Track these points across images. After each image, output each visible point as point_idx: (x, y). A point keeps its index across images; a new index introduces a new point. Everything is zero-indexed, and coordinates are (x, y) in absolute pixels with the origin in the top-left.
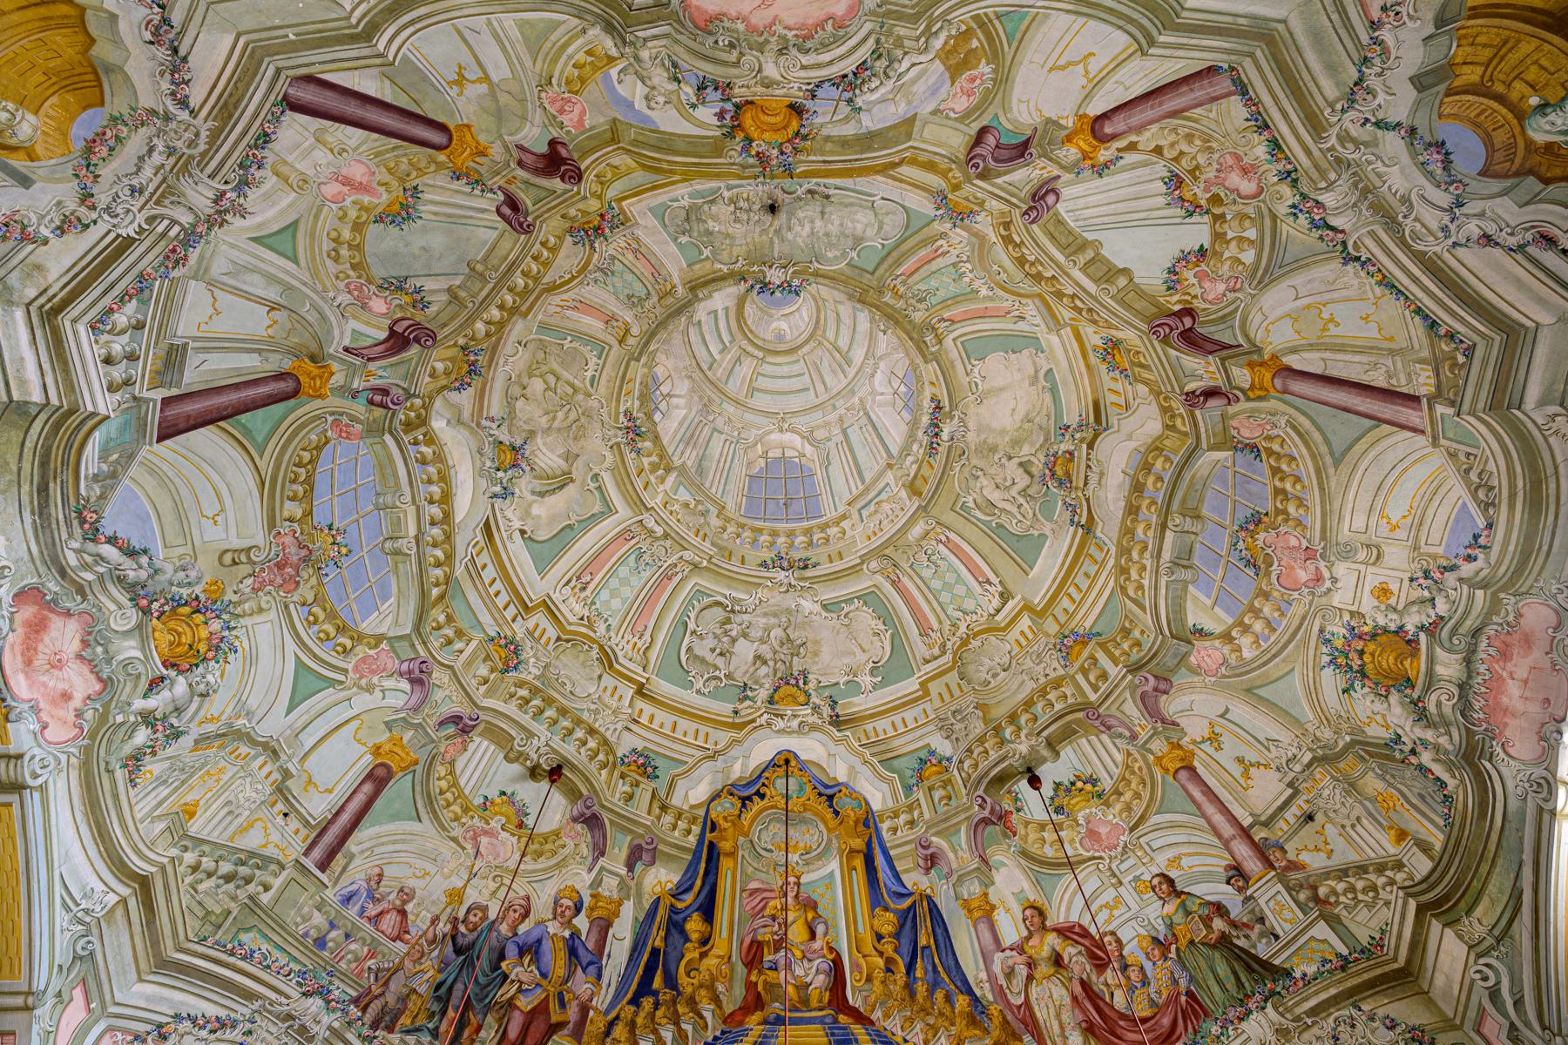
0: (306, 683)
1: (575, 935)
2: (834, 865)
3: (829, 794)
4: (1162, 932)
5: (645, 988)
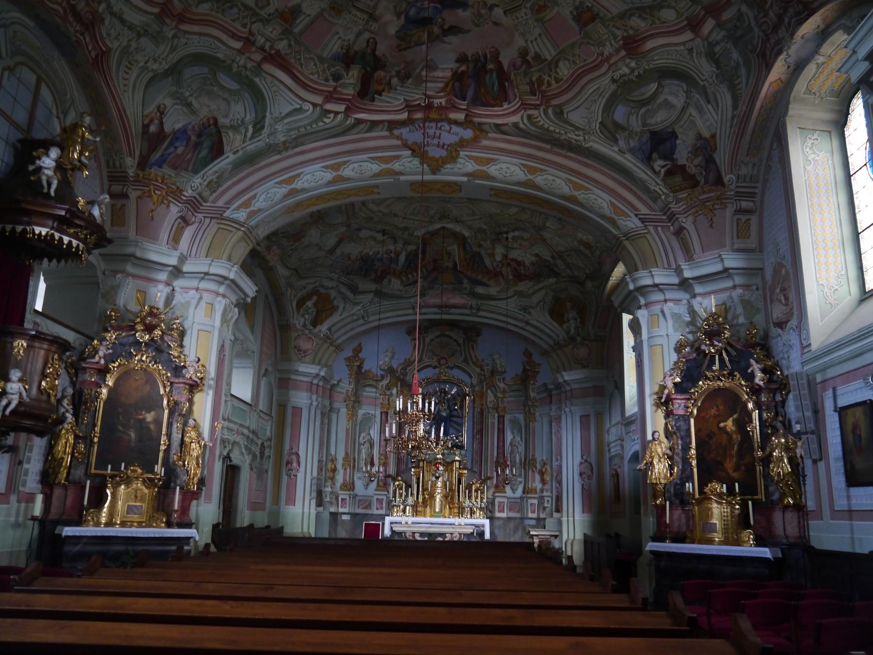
1: (391, 257)
2: (456, 247)
3: (455, 235)
4: (534, 262)
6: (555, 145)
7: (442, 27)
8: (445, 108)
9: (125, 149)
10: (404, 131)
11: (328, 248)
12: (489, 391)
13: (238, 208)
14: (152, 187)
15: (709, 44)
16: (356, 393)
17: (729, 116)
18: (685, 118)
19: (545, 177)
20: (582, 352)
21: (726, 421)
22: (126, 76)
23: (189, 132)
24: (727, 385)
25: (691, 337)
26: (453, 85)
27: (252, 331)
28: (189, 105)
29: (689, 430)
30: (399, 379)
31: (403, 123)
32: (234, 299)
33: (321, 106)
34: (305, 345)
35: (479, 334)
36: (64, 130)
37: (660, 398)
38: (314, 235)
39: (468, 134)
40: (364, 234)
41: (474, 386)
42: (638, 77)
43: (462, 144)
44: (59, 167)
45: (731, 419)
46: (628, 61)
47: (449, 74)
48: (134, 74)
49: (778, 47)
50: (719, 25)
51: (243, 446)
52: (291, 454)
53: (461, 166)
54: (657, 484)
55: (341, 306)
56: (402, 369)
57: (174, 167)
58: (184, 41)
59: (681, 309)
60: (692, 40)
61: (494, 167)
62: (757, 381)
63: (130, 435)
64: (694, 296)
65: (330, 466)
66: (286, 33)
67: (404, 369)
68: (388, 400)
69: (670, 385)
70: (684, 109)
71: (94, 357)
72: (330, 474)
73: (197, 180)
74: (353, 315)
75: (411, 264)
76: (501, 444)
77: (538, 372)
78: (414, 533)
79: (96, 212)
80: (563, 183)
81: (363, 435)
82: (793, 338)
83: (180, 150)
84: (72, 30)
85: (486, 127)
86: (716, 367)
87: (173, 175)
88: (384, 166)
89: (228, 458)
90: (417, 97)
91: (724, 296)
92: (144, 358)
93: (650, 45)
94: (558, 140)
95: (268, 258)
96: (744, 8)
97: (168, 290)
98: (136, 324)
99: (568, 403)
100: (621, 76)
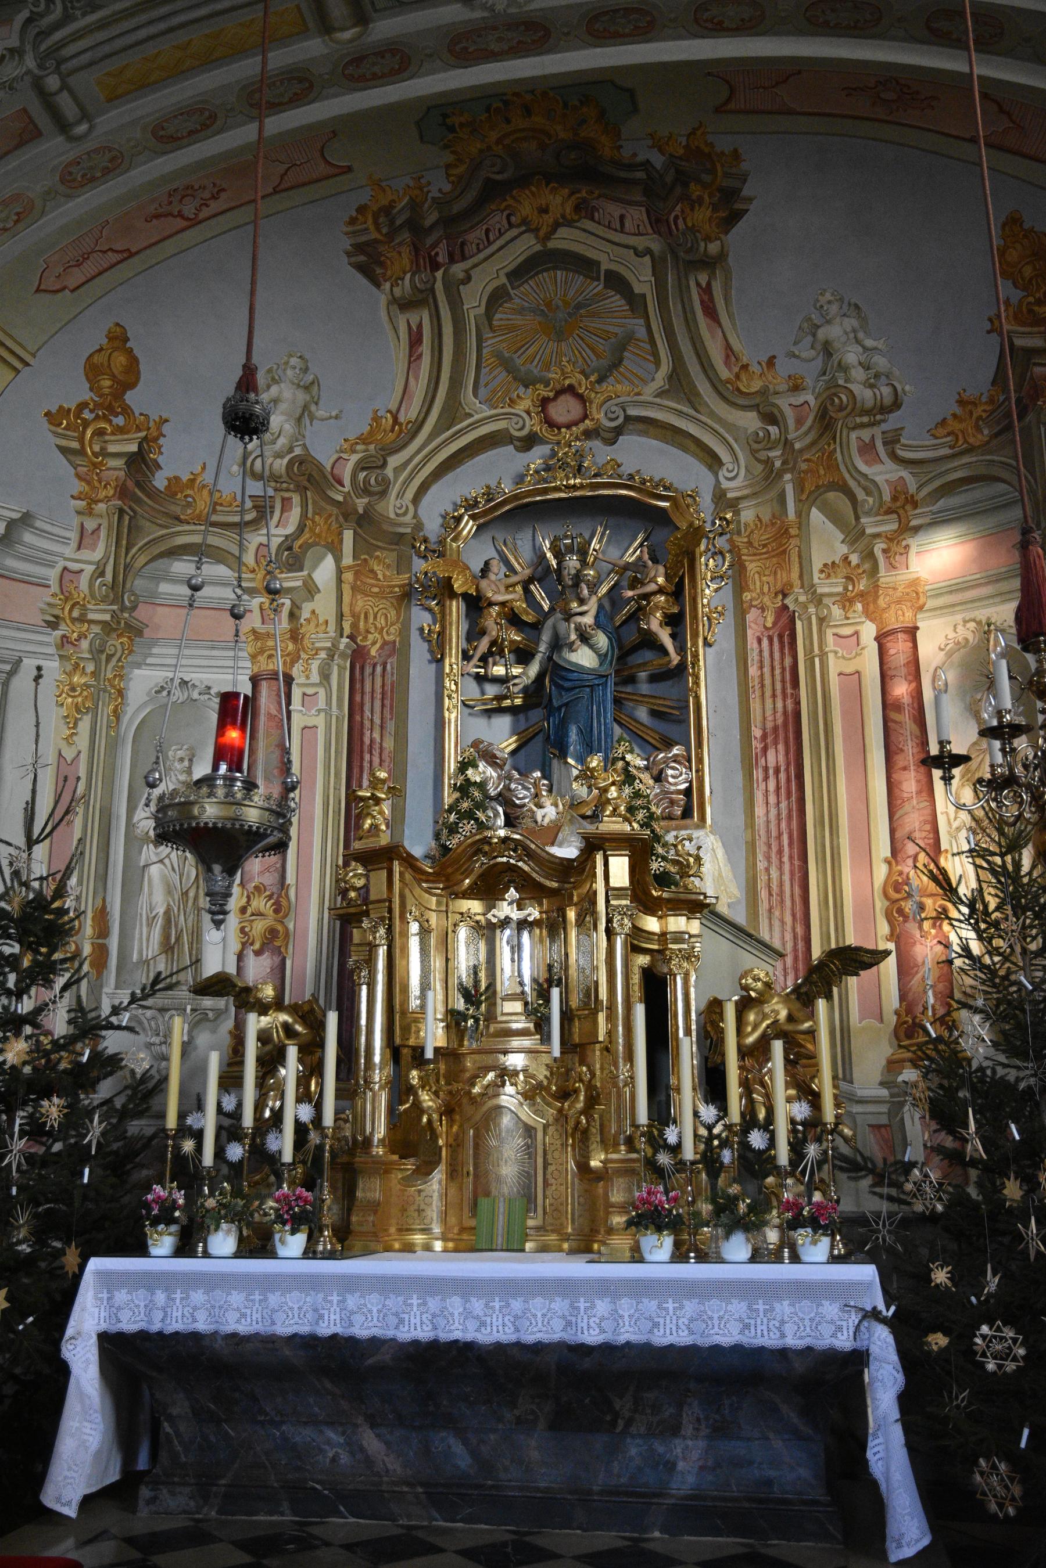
12: (816, 515)
16: (117, 591)
30: (347, 512)
41: (734, 505)
56: (361, 466)
67: (372, 464)
68: (293, 616)
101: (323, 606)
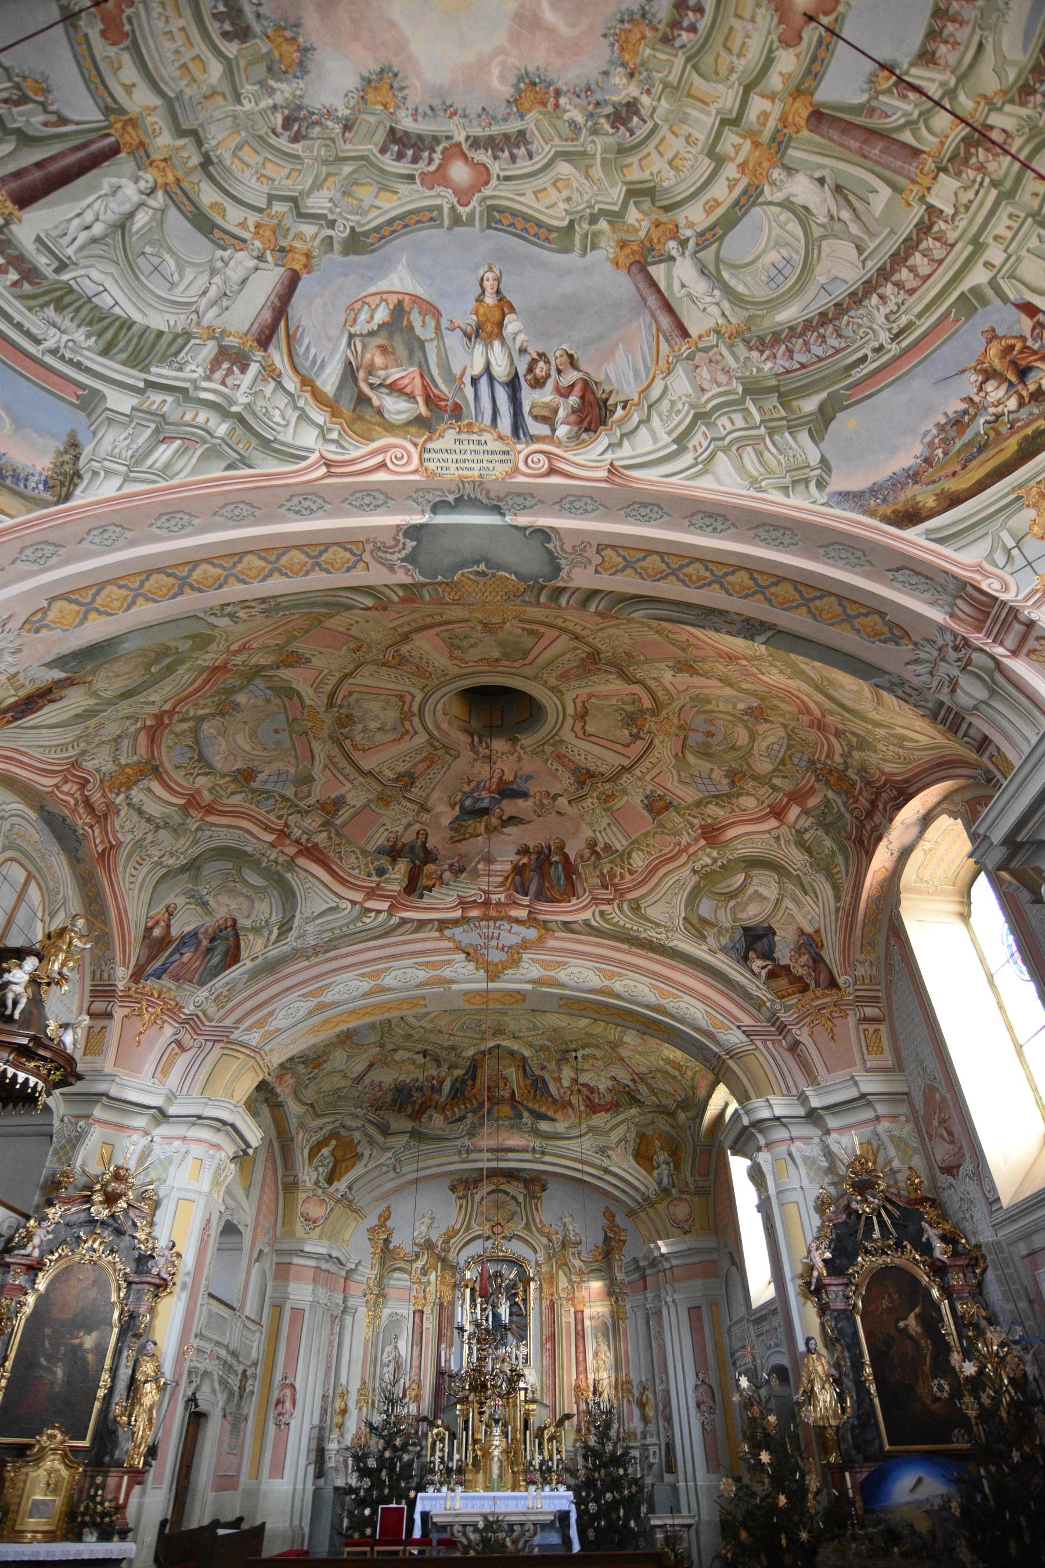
0: (349, 1058)
2: (513, 1069)
3: (512, 1053)
5: (455, 1096)
6: (633, 945)
7: (500, 818)
8: (506, 904)
9: (118, 957)
10: (457, 931)
11: (354, 1075)
13: (249, 1029)
14: (144, 1003)
15: (797, 831)
16: (380, 1284)
17: (833, 908)
18: (781, 913)
19: (625, 982)
20: (681, 1211)
21: (906, 1318)
22: (134, 872)
23: (201, 936)
24: (897, 1261)
25: (832, 1190)
26: (513, 880)
27: (247, 1196)
28: (204, 904)
29: (856, 1333)
30: (439, 1256)
31: (456, 922)
32: (230, 1149)
33: (361, 903)
34: (316, 1211)
35: (544, 1188)
36: (49, 936)
37: (808, 1284)
38: (339, 1058)
39: (532, 933)
40: (400, 1055)
42: (722, 867)
43: (525, 945)
44: (34, 981)
45: (912, 1315)
46: (708, 850)
47: (508, 867)
48: (145, 869)
49: (875, 834)
50: (806, 812)
51: (216, 1378)
52: (284, 1386)
53: (524, 972)
54: (825, 1427)
55: (367, 1153)
57: (177, 978)
58: (209, 833)
59: (814, 1150)
60: (778, 828)
61: (563, 972)
62: (937, 1254)
63: (55, 1373)
64: (828, 1132)
65: (339, 1404)
66: (326, 824)
67: (446, 1242)
69: (820, 1264)
70: (778, 902)
71: (24, 1247)
72: (338, 1419)
73: (203, 993)
74: (382, 1165)
75: (459, 1092)
76: (581, 1358)
77: (624, 1241)
78: (464, 1526)
79: (68, 1038)
80: (647, 990)
81: (388, 1349)
82: (971, 1188)
83: (186, 958)
84: (80, 822)
85: (552, 926)
86: (877, 1235)
87: (173, 987)
88: (433, 973)
89: (192, 1400)
90: (472, 892)
91: (868, 1130)
92: (96, 1246)
93: (731, 833)
94: (637, 938)
95: (279, 1090)
96: (830, 795)
97: (144, 1141)
98: (94, 1192)
99: (669, 1288)
100: (703, 867)
101: (432, 1288)
